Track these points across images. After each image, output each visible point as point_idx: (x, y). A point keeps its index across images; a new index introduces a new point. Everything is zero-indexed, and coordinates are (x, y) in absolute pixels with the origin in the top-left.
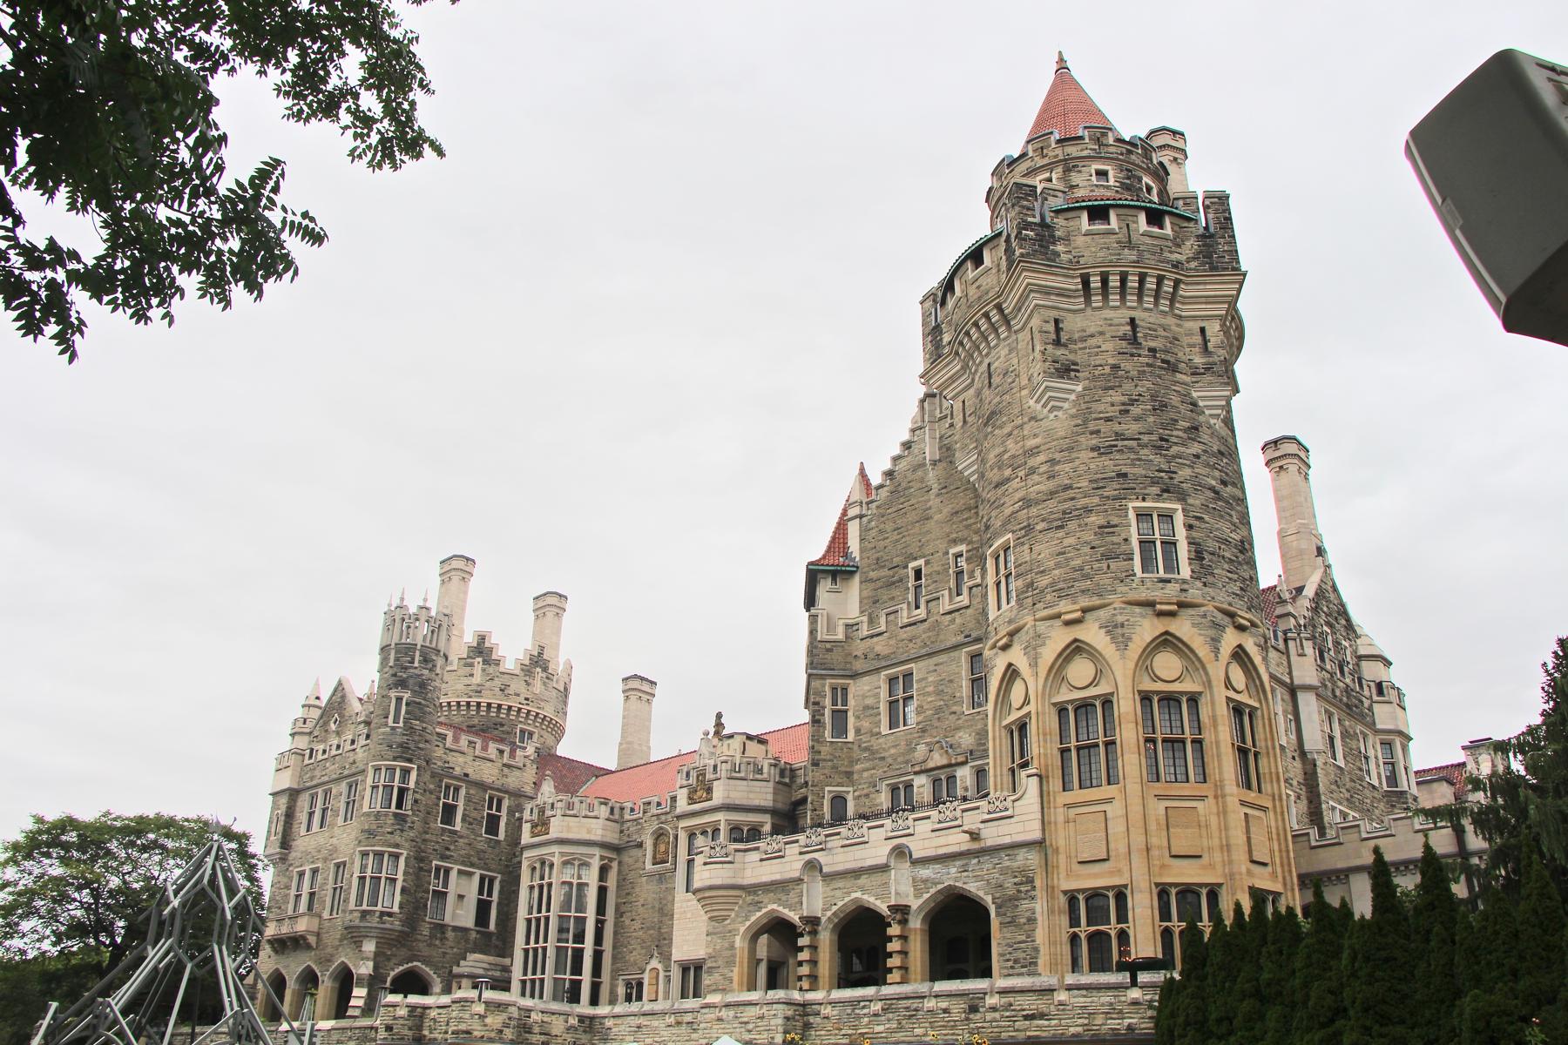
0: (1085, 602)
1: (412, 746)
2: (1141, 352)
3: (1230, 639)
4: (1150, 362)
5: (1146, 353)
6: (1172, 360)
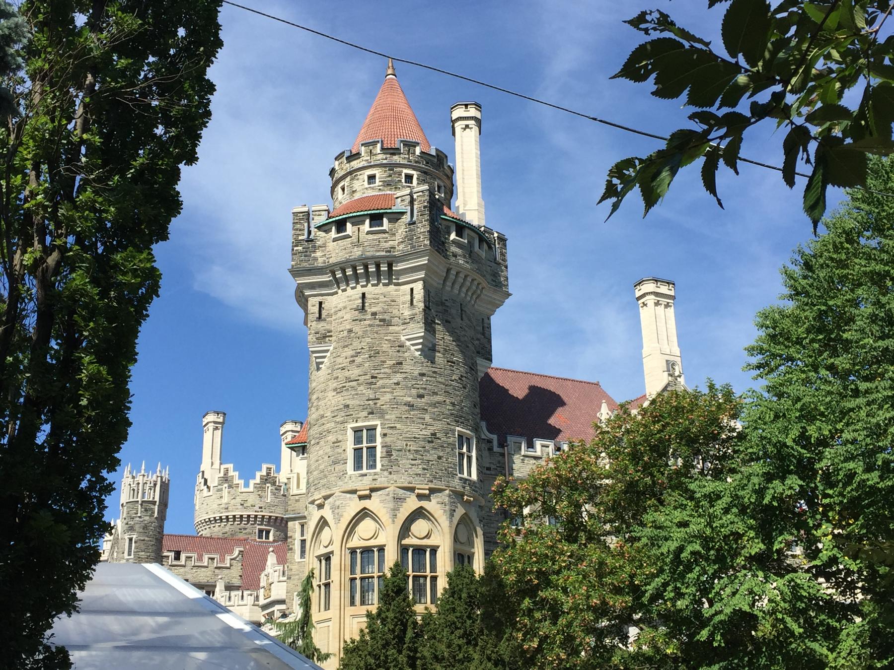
0: (325, 492)
4: (371, 323)
5: (370, 317)
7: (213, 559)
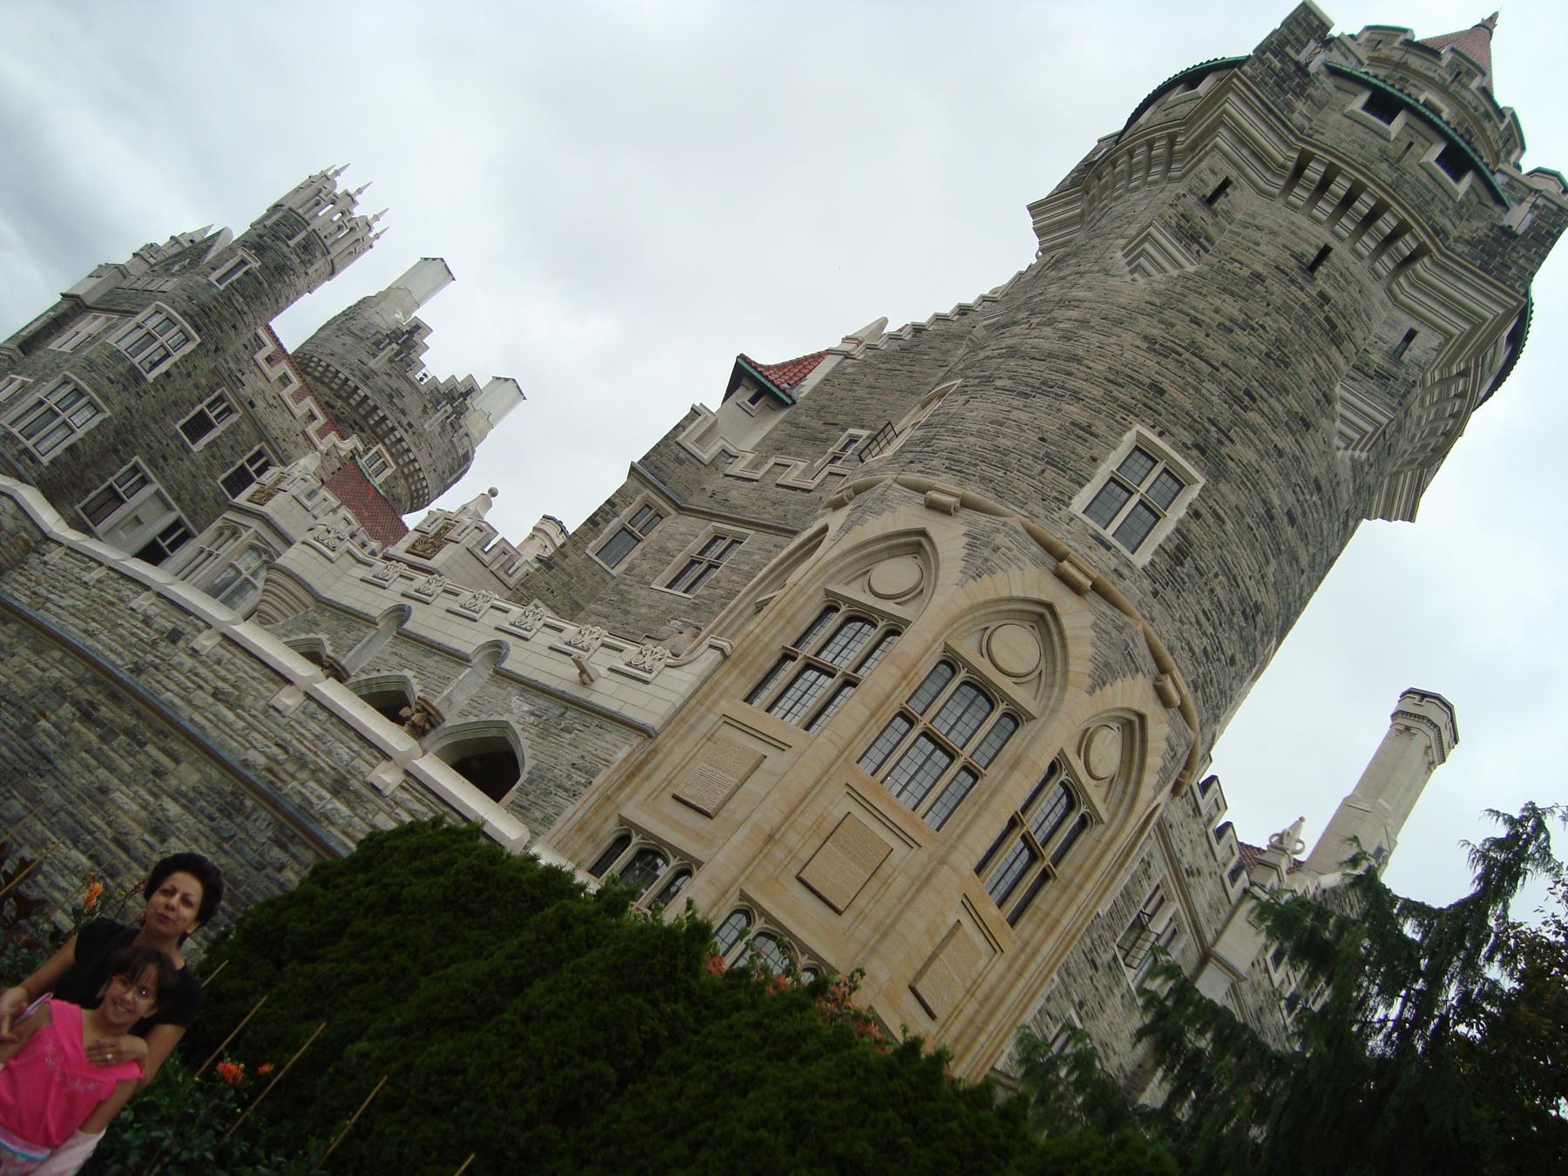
0: (973, 492)
1: (214, 317)
2: (1308, 287)
3: (1134, 692)
4: (1310, 305)
6: (1342, 328)
7: (312, 417)
